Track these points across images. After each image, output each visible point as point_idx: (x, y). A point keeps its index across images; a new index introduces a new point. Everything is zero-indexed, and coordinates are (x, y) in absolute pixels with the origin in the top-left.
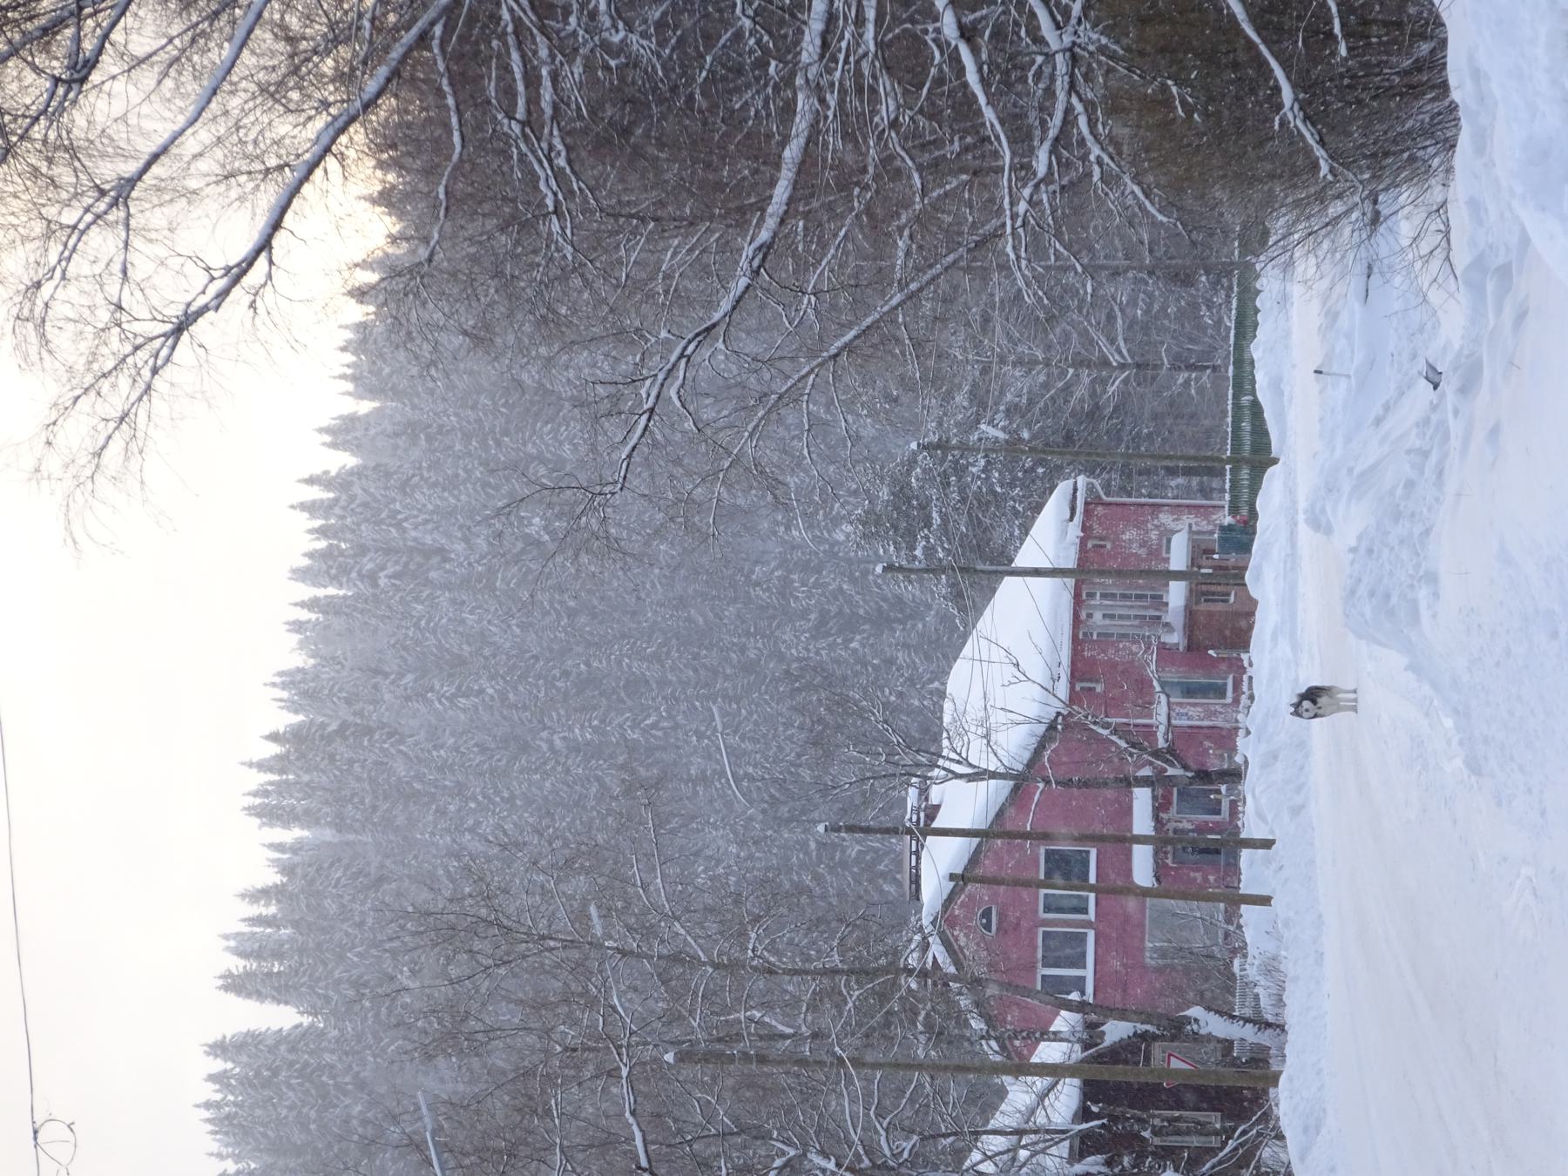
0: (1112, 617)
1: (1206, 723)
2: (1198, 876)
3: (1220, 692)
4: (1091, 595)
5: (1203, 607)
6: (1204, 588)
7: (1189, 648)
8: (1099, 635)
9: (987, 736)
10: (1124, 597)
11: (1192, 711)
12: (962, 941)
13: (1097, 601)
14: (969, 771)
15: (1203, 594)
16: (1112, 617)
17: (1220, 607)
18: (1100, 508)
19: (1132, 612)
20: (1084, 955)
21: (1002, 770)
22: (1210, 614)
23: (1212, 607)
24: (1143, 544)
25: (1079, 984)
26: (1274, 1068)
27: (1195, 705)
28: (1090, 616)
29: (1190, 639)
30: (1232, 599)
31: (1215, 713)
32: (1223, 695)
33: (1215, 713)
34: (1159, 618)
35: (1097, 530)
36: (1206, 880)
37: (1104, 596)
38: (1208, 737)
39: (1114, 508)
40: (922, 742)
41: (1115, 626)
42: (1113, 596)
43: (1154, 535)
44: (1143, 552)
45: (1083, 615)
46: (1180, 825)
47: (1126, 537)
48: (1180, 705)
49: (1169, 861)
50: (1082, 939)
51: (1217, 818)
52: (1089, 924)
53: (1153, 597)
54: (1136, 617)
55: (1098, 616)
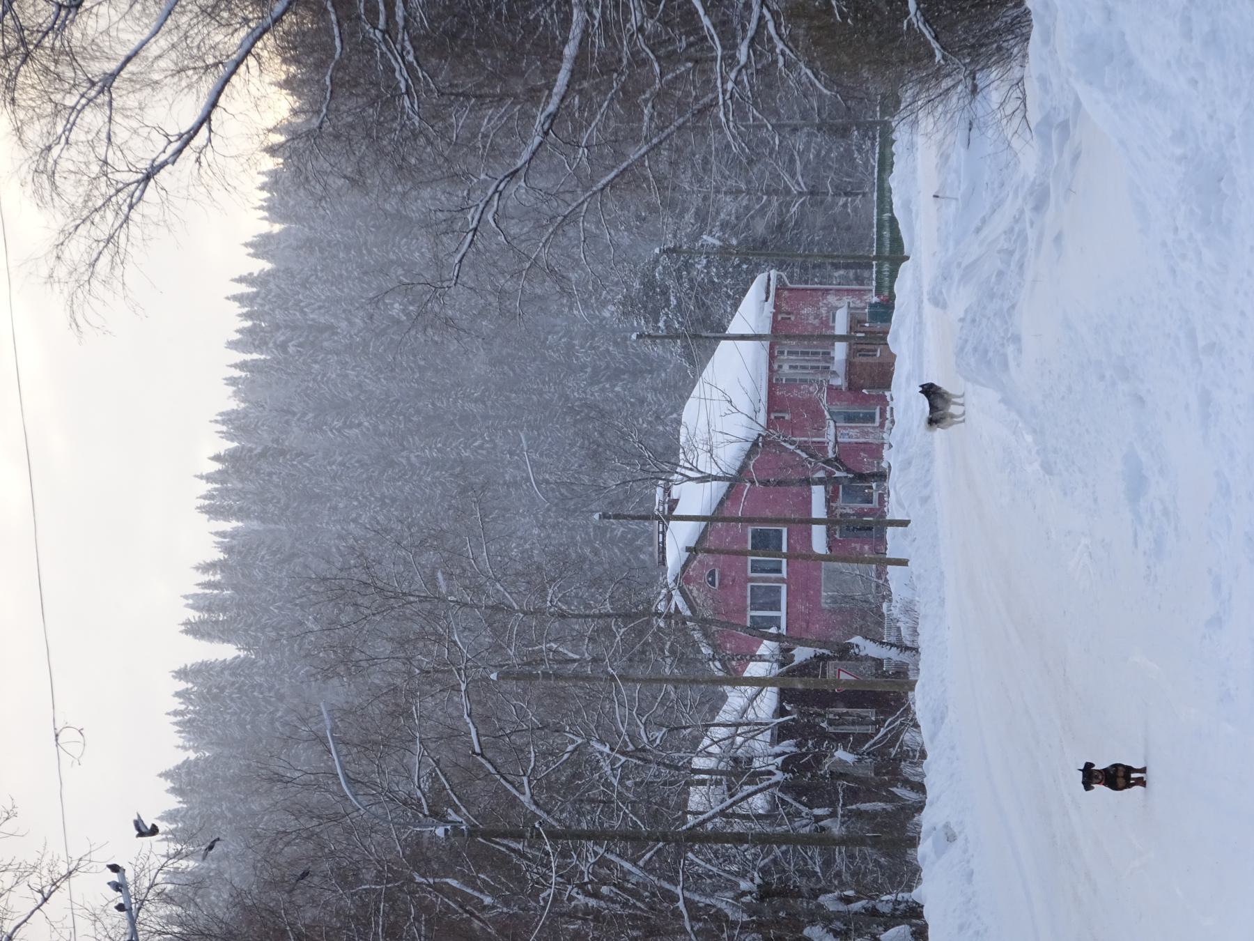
0: (796, 367)
2: (858, 546)
3: (871, 418)
4: (782, 353)
5: (858, 359)
6: (860, 347)
7: (849, 388)
9: (710, 451)
10: (804, 353)
11: (852, 432)
12: (695, 593)
13: (785, 357)
14: (699, 475)
16: (796, 367)
17: (870, 360)
19: (809, 364)
20: (779, 601)
21: (721, 474)
23: (864, 360)
24: (817, 316)
25: (775, 621)
26: (912, 678)
28: (780, 367)
31: (867, 433)
32: (873, 420)
33: (867, 433)
35: (785, 307)
36: (862, 548)
37: (790, 353)
38: (863, 450)
40: (664, 456)
41: (798, 374)
42: (796, 353)
43: (823, 311)
44: (816, 322)
45: (776, 367)
47: (805, 311)
48: (844, 428)
49: (837, 536)
50: (778, 590)
52: (782, 580)
53: (824, 353)
54: (812, 368)
55: (786, 367)
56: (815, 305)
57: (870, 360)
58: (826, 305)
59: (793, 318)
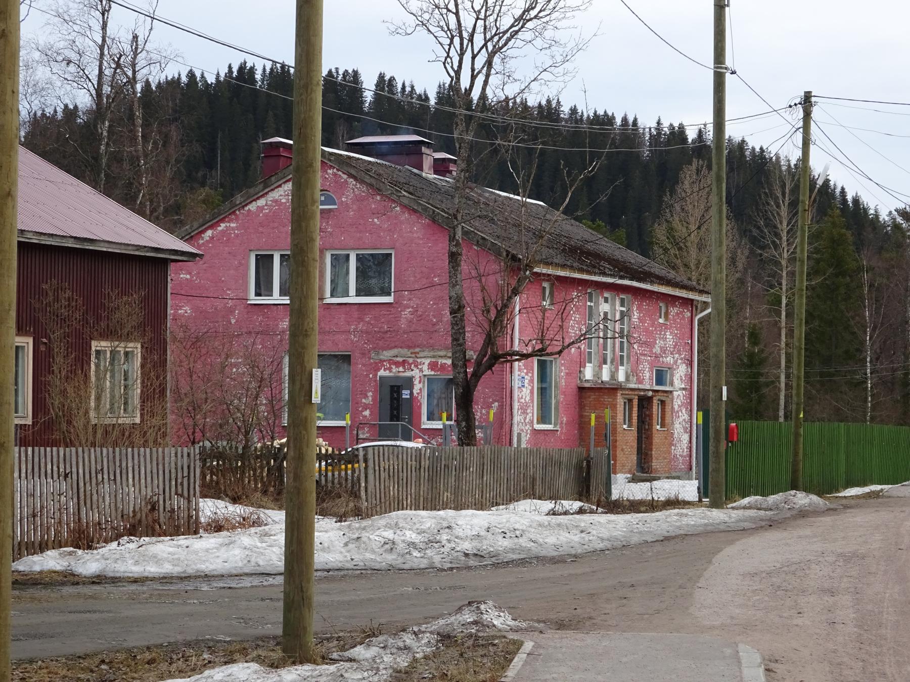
1: (516, 406)
2: (369, 400)
4: (622, 305)
5: (620, 401)
6: (635, 402)
7: (581, 389)
8: (590, 307)
11: (526, 392)
13: (618, 308)
15: (630, 401)
17: (620, 418)
18: (689, 314)
22: (614, 407)
24: (664, 350)
27: (532, 392)
28: (606, 300)
29: (590, 389)
30: (625, 427)
31: (525, 412)
33: (525, 412)
34: (605, 363)
38: (501, 407)
39: (689, 327)
43: (669, 360)
44: (657, 349)
46: (416, 382)
48: (532, 381)
51: (424, 417)
53: (622, 357)
55: (604, 307)
56: (676, 348)
57: (620, 418)
58: (676, 362)
59: (661, 321)
